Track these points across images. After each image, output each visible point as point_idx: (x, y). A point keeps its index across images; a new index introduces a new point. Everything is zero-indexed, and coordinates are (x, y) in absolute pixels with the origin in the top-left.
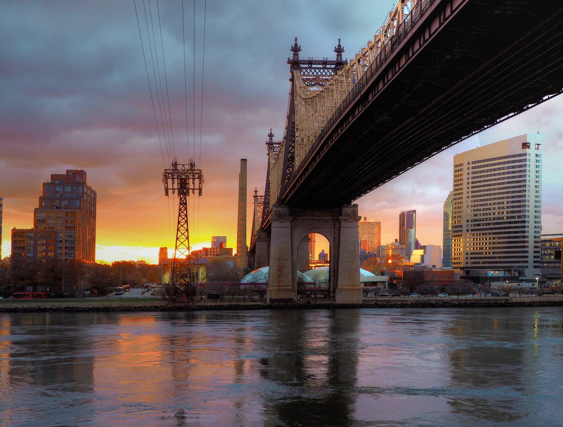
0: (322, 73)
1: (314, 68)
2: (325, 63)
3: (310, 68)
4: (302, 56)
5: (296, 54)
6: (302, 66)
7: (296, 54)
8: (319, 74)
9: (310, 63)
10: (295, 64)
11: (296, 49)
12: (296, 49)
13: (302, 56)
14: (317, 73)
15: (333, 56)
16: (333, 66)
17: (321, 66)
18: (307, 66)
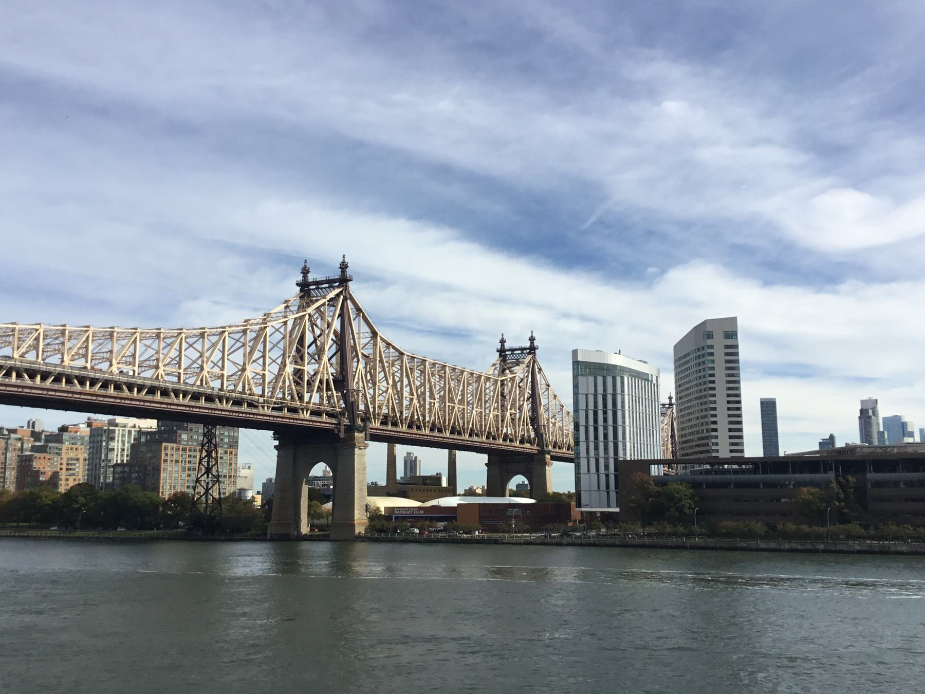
0: (521, 357)
1: (322, 288)
2: (330, 282)
3: (317, 289)
4: (311, 277)
5: (305, 277)
6: (311, 287)
7: (305, 277)
8: (519, 357)
9: (317, 283)
10: (304, 286)
11: (305, 272)
12: (305, 272)
13: (311, 277)
14: (513, 356)
15: (337, 274)
16: (337, 284)
17: (327, 285)
18: (314, 287)
